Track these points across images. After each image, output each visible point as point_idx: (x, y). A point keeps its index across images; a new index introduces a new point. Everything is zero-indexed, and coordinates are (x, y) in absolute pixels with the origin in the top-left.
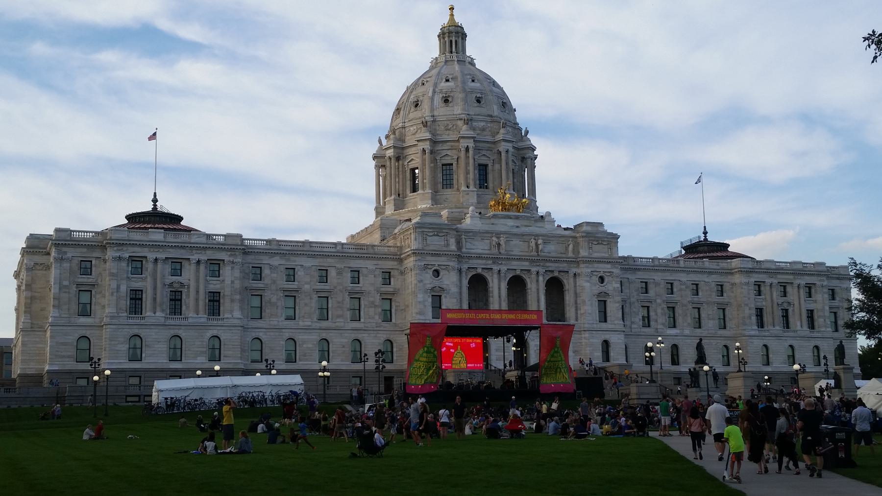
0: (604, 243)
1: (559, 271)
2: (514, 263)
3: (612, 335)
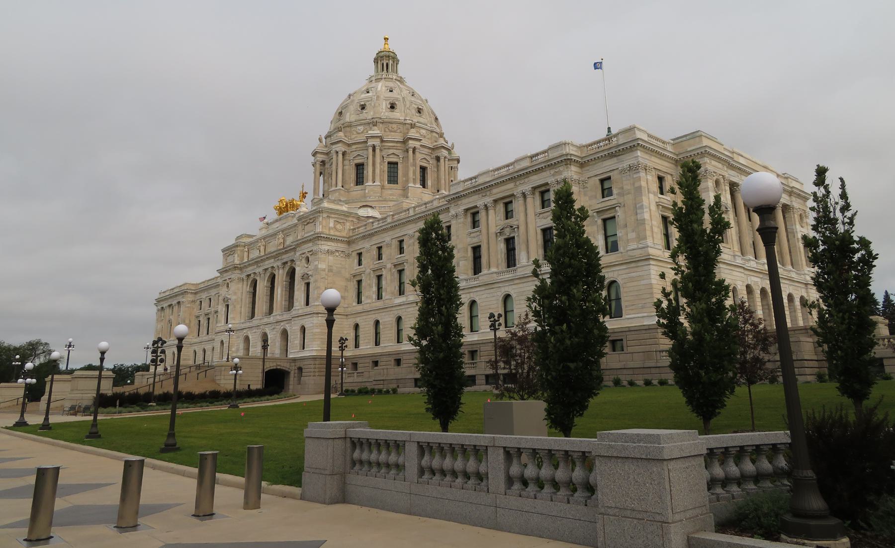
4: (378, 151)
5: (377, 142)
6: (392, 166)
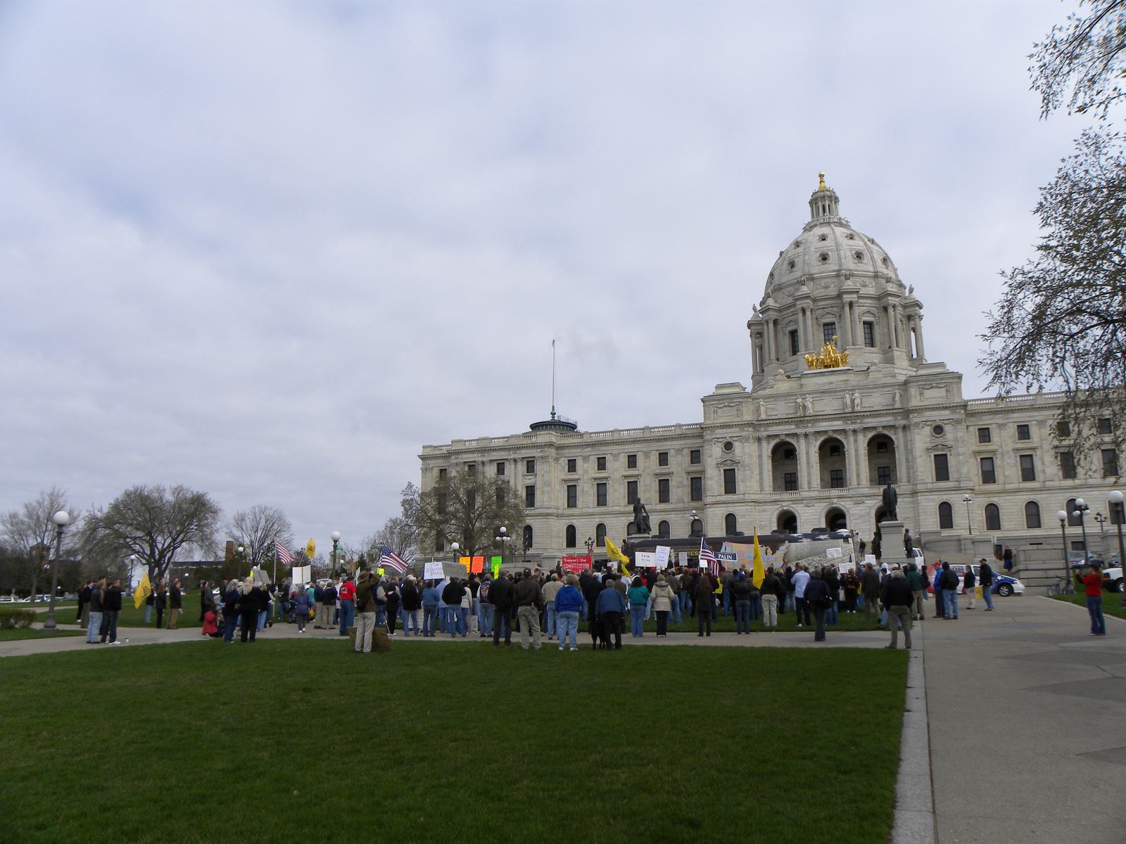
0: (940, 386)
1: (883, 427)
2: (822, 424)
3: (952, 496)
4: (808, 313)
5: (807, 303)
6: (830, 327)
